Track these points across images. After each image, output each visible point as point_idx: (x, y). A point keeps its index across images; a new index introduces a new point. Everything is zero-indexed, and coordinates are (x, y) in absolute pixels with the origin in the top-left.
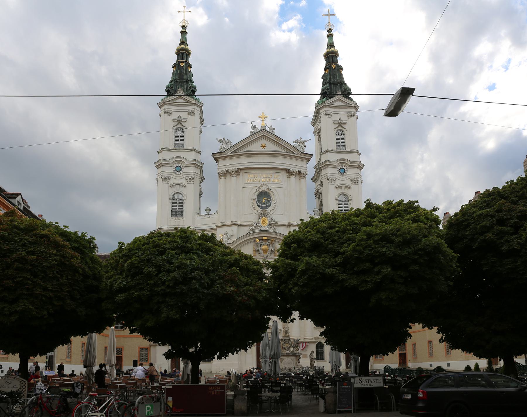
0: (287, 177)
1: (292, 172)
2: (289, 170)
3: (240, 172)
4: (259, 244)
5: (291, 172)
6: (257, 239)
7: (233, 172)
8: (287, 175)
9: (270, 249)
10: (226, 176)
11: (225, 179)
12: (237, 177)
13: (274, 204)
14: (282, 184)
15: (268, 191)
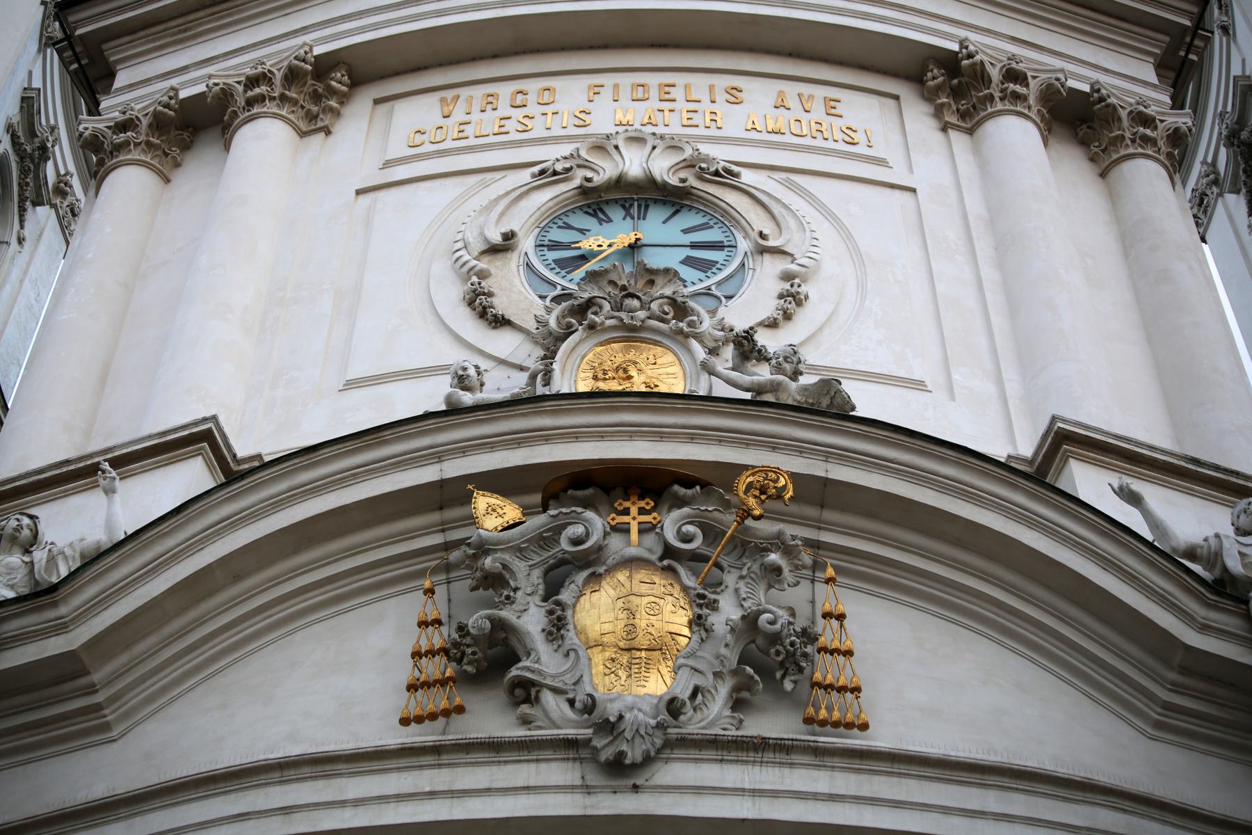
0: (945, 128)
1: (995, 74)
2: (950, 63)
3: (344, 99)
4: (520, 566)
5: (980, 76)
6: (482, 501)
7: (252, 82)
8: (938, 113)
9: (728, 612)
10: (177, 165)
11: (167, 181)
12: (303, 134)
13: (788, 277)
14: (880, 162)
15: (693, 182)
